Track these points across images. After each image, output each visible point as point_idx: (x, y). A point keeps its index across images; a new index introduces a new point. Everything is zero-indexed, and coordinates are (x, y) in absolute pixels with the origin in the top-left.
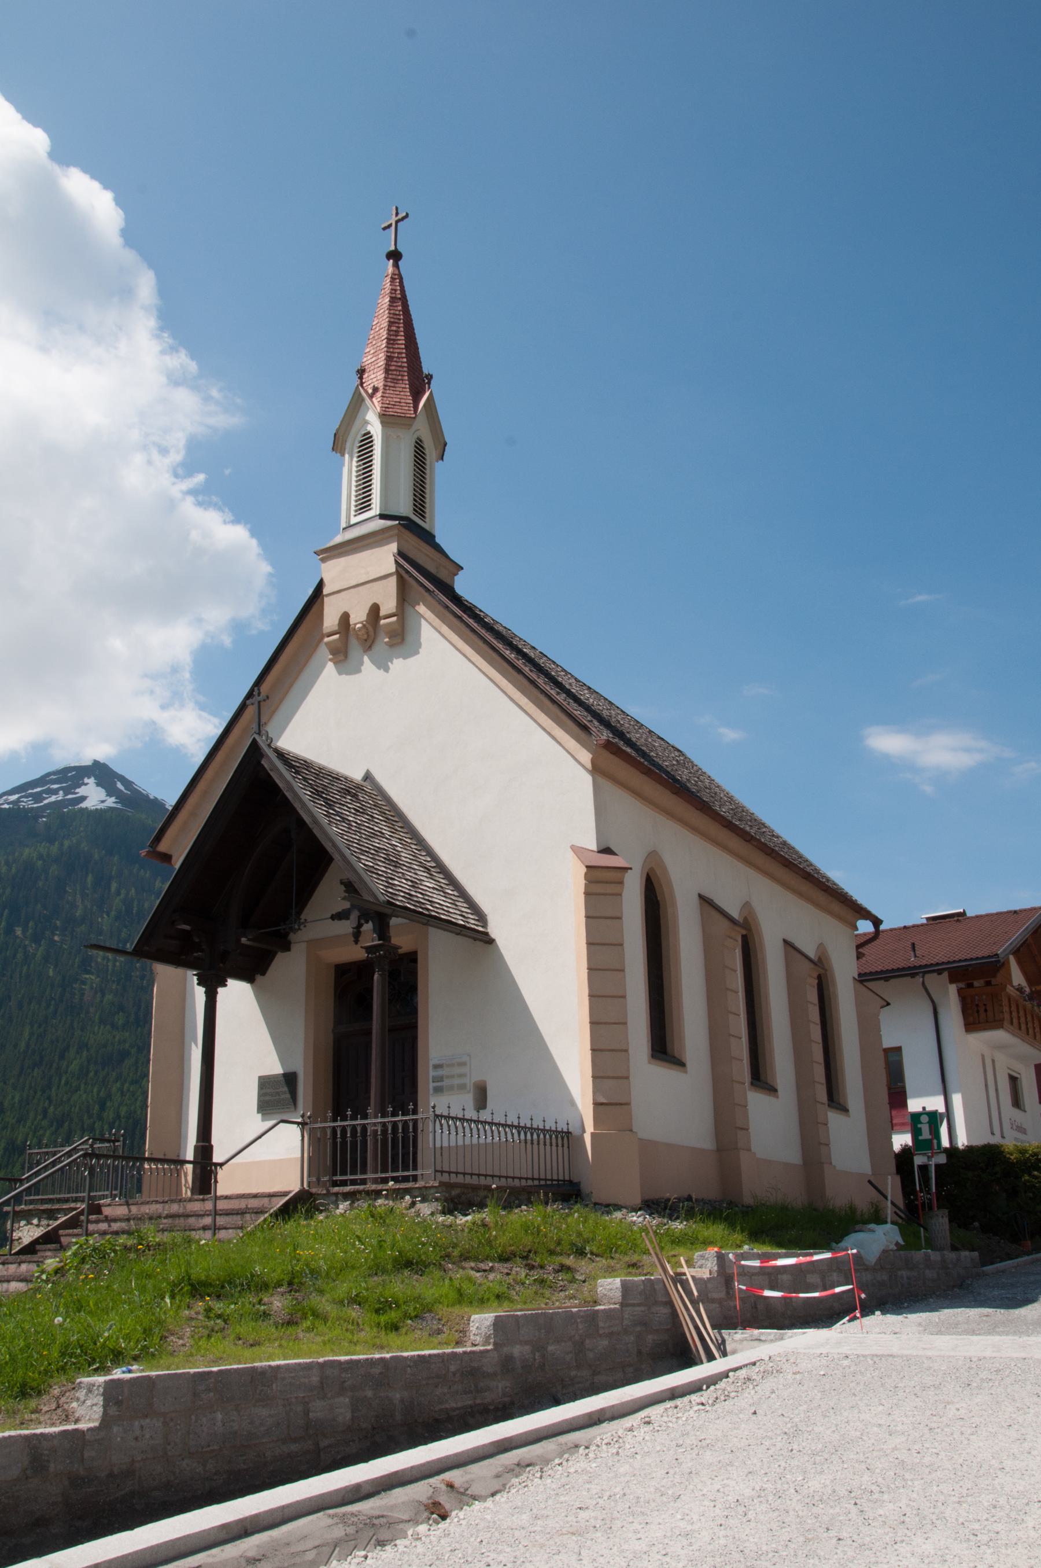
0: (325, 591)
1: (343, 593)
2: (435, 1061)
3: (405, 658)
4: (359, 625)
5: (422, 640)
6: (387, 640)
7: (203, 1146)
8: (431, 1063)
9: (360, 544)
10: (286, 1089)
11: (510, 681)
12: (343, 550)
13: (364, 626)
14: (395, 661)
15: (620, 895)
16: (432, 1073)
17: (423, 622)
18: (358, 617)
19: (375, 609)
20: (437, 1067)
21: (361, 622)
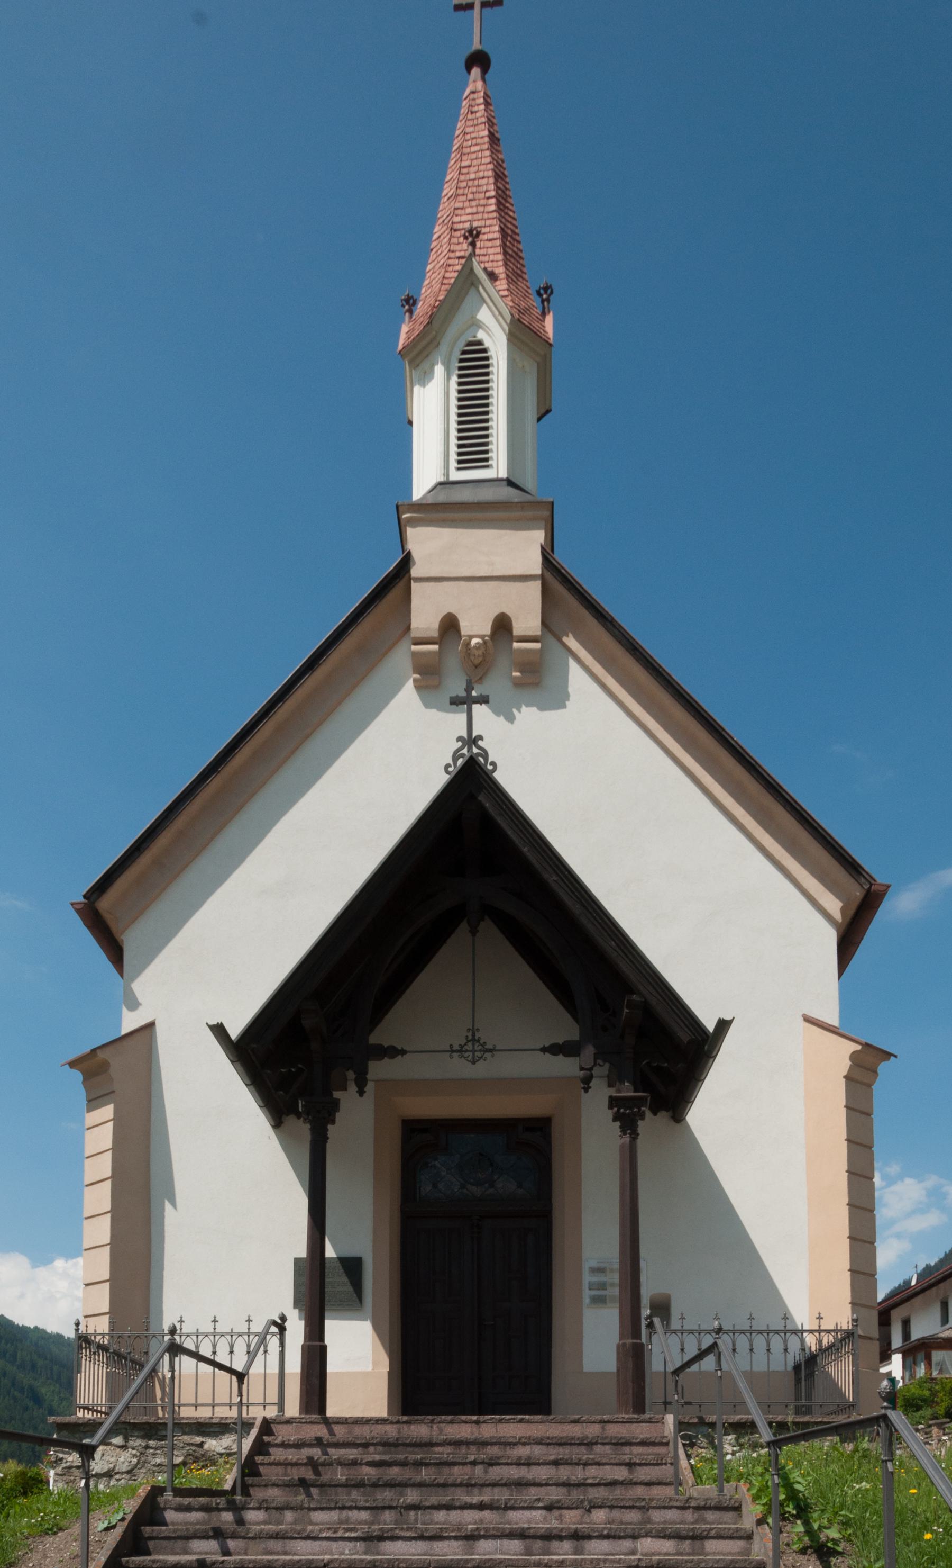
0: (415, 572)
1: (445, 584)
2: (594, 1264)
3: (542, 708)
4: (474, 641)
5: (570, 690)
6: (516, 674)
7: (309, 1346)
8: (586, 1266)
9: (479, 515)
10: (345, 1279)
11: (717, 780)
12: (451, 515)
13: (485, 642)
14: (524, 708)
15: (869, 1086)
16: (587, 1278)
17: (572, 664)
18: (476, 626)
19: (502, 625)
20: (594, 1271)
21: (482, 637)
